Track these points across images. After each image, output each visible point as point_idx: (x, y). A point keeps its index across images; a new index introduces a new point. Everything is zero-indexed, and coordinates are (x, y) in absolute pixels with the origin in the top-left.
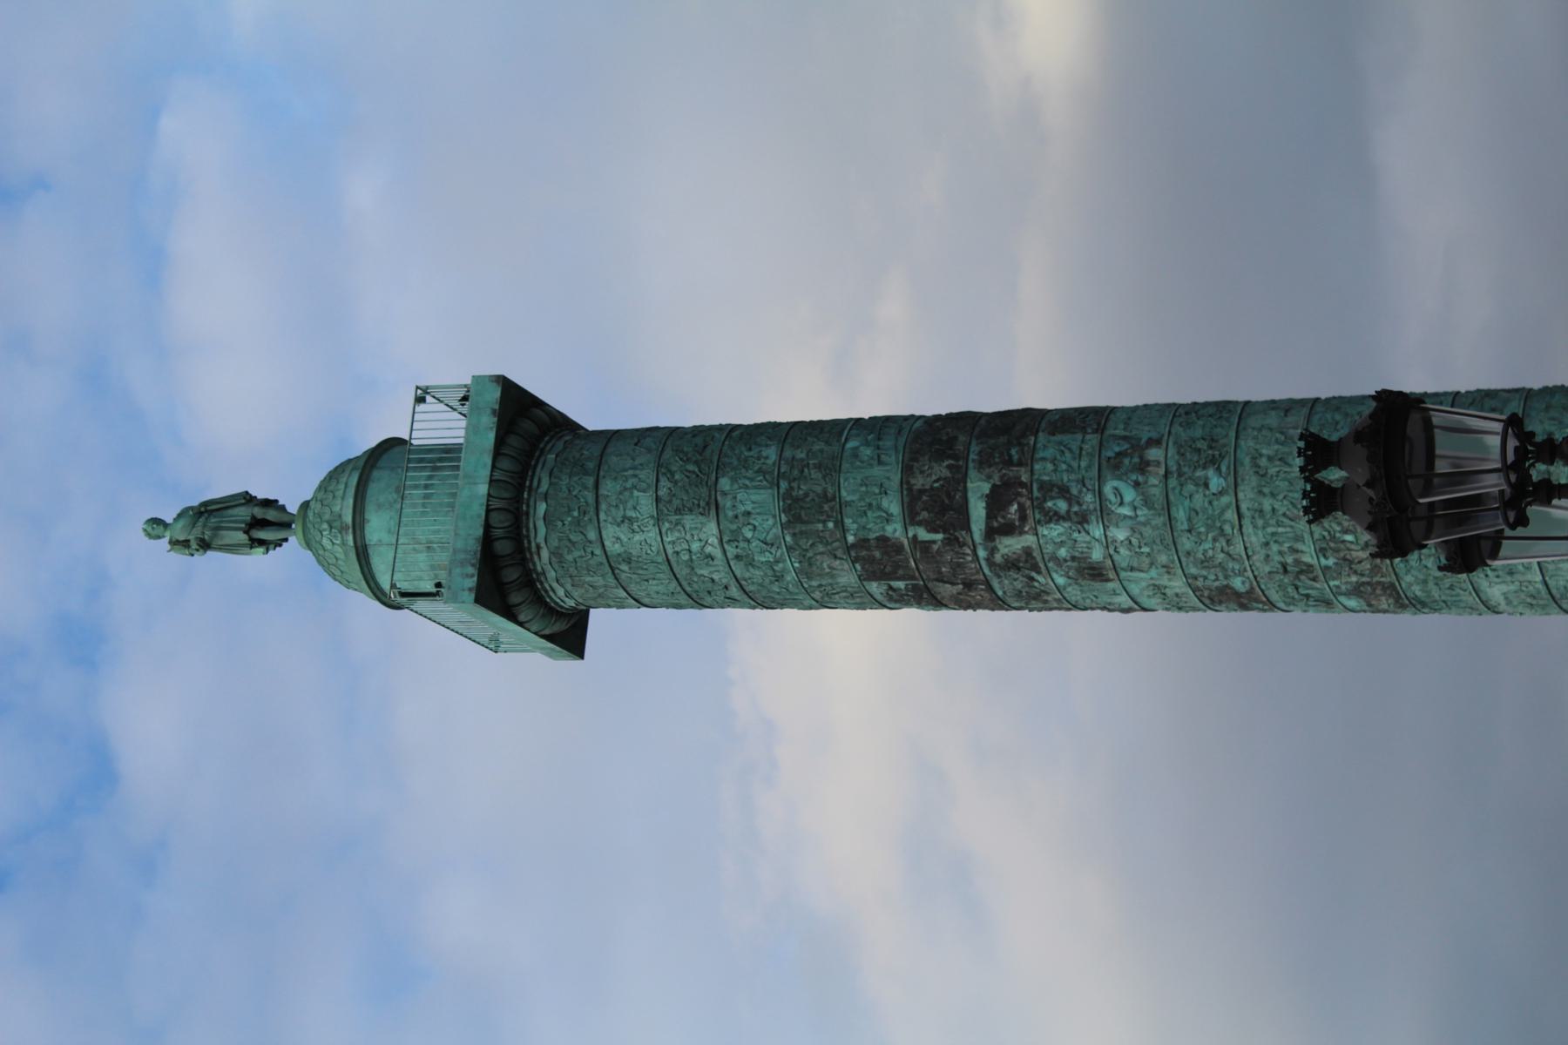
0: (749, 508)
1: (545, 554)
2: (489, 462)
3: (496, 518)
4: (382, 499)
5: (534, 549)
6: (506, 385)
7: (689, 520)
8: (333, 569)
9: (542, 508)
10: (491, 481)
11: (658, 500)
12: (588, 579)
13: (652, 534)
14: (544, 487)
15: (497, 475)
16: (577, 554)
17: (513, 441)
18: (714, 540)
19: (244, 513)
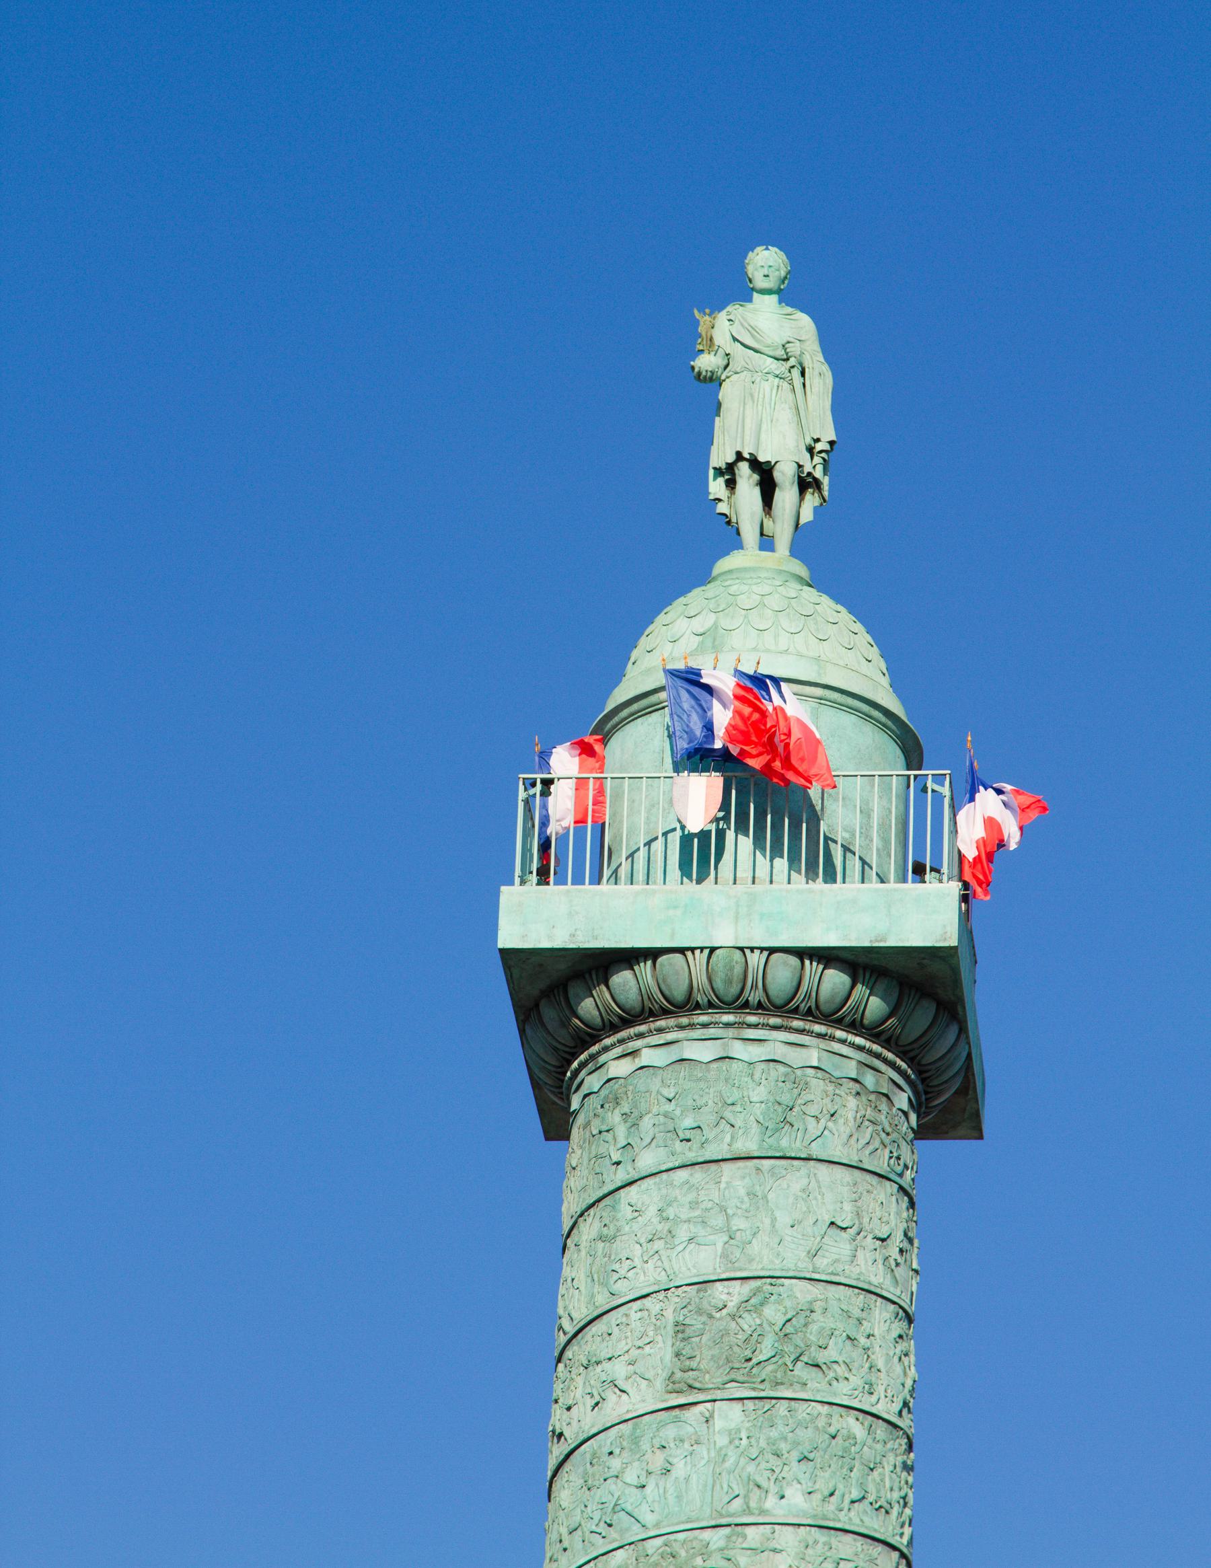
0: (680, 1469)
7: (662, 1352)
9: (702, 1052)
10: (742, 949)
14: (739, 1050)
15: (755, 959)
17: (835, 980)
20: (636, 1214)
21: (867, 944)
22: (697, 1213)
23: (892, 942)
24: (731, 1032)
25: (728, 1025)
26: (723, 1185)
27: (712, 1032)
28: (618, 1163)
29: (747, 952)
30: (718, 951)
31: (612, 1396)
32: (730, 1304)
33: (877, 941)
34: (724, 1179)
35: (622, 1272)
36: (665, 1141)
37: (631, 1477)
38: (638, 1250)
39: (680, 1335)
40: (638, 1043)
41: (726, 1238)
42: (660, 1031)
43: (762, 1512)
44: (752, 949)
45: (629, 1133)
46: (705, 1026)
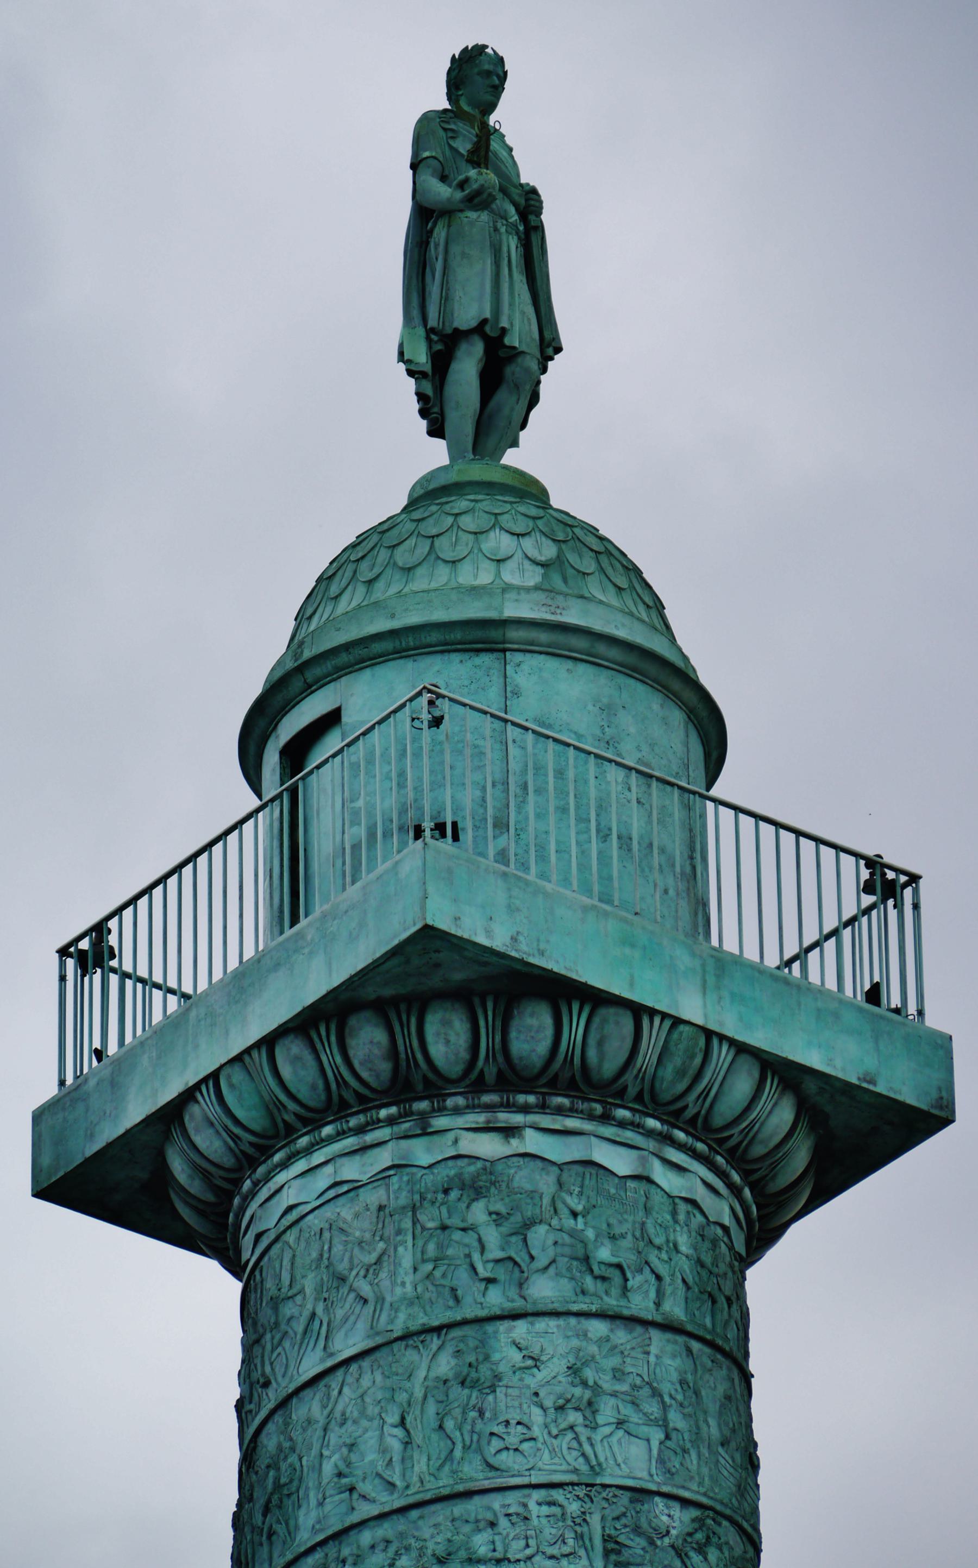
1: (489, 1146)
3: (619, 1028)
4: (626, 721)
5: (505, 1118)
6: (917, 1123)
8: (375, 538)
9: (620, 1162)
10: (709, 1034)
11: (640, 1494)
12: (406, 1257)
13: (552, 1462)
15: (722, 1055)
16: (492, 1236)
19: (520, 331)
21: (854, 1081)
22: (625, 1387)
23: (880, 1088)
24: (651, 1145)
25: (650, 1133)
28: (490, 1281)
29: (715, 1042)
30: (682, 1027)
32: (674, 1532)
33: (865, 1080)
34: (654, 1350)
35: (512, 1440)
36: (569, 1269)
38: (537, 1416)
39: (613, 1557)
40: (518, 1119)
41: (662, 1436)
44: (722, 1038)
46: (622, 1124)
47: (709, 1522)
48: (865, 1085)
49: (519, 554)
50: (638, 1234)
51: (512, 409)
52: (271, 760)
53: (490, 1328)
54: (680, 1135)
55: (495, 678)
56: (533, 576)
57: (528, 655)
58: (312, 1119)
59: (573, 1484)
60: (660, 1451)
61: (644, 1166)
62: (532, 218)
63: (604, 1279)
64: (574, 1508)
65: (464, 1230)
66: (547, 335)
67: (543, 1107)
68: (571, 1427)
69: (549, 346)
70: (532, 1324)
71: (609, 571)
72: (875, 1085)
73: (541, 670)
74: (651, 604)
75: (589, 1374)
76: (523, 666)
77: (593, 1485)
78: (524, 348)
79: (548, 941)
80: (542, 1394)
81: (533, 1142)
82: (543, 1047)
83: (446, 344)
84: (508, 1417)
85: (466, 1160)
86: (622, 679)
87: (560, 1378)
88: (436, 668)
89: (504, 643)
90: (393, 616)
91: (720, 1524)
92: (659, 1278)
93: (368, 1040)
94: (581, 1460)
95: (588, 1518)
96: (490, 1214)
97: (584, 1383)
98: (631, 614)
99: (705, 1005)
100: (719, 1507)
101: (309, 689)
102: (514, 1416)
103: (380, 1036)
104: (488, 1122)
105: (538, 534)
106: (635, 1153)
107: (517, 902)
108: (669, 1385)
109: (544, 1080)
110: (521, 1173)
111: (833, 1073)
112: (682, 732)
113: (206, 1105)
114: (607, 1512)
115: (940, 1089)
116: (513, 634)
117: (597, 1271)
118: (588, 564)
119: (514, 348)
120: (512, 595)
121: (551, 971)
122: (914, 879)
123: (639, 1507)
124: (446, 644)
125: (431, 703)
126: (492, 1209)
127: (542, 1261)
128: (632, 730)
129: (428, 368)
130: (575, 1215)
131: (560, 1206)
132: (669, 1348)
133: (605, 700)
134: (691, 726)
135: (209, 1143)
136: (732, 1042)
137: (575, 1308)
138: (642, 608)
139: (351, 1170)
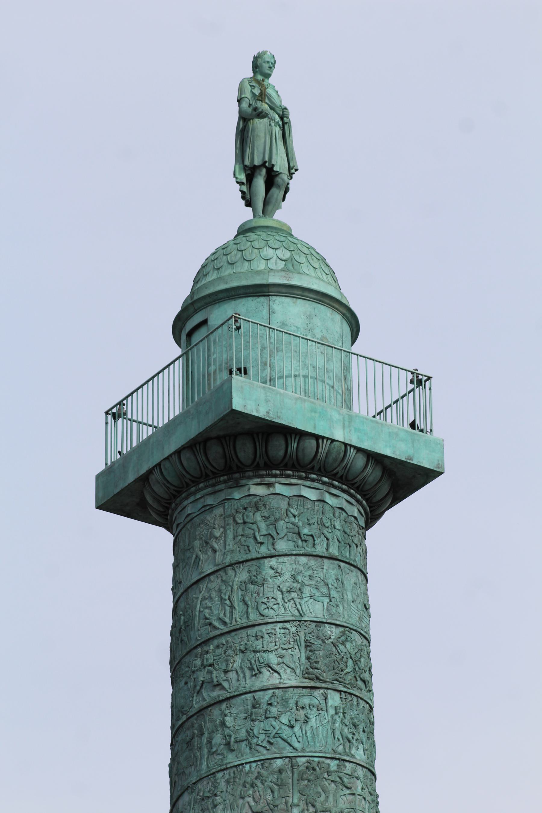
0: (313, 722)
1: (260, 491)
2: (366, 445)
4: (317, 321)
7: (299, 655)
9: (312, 495)
10: (346, 445)
11: (319, 623)
15: (352, 452)
18: (275, 680)
19: (280, 164)
20: (277, 574)
21: (404, 459)
22: (313, 582)
23: (415, 462)
24: (325, 488)
25: (324, 483)
26: (325, 571)
27: (316, 485)
28: (262, 543)
29: (348, 447)
30: (335, 443)
31: (266, 673)
32: (332, 637)
33: (408, 459)
34: (325, 567)
36: (292, 537)
37: (284, 719)
39: (309, 648)
40: (273, 480)
41: (328, 600)
42: (288, 476)
43: (353, 756)
44: (351, 446)
45: (268, 528)
46: (313, 480)
47: (347, 632)
48: (408, 461)
49: (275, 257)
50: (319, 522)
51: (278, 195)
52: (184, 337)
53: (261, 561)
54: (336, 483)
55: (265, 306)
56: (281, 265)
57: (278, 297)
58: (196, 481)
59: (293, 621)
60: (327, 606)
61: (322, 496)
62: (285, 119)
63: (306, 541)
64: (293, 630)
65: (252, 523)
66: (292, 165)
67: (281, 476)
68: (293, 599)
69: (292, 170)
70: (278, 559)
71: (311, 262)
72: (412, 460)
73: (283, 303)
74: (328, 272)
75: (300, 578)
76: (276, 302)
77: (301, 621)
78: (281, 171)
79: (281, 413)
80: (281, 587)
81: (279, 489)
82: (281, 453)
83: (251, 171)
84: (268, 596)
85: (253, 497)
86: (315, 305)
87: (288, 580)
88: (243, 303)
89: (268, 293)
90: (227, 283)
91: (351, 633)
92: (328, 539)
93: (215, 451)
94: (296, 611)
95: (299, 633)
96: (262, 517)
97: (298, 582)
98: (319, 278)
99: (344, 434)
100: (351, 627)
101: (196, 311)
102: (271, 595)
103: (220, 450)
104: (261, 481)
105: (283, 248)
106: (318, 491)
107: (269, 398)
108: (331, 580)
109: (282, 465)
110: (274, 501)
111: (395, 457)
112: (339, 323)
113: (156, 475)
114: (306, 631)
115: (438, 460)
116: (272, 289)
117: (303, 538)
118: (303, 259)
119: (278, 172)
120: (272, 274)
121: (282, 424)
122: (429, 378)
123: (319, 628)
124: (246, 294)
125: (236, 321)
126: (262, 515)
127: (282, 535)
128: (319, 324)
129: (244, 181)
130: (294, 516)
131: (289, 513)
132: (332, 566)
133: (308, 313)
134: (344, 320)
135: (159, 490)
136: (355, 447)
137: (294, 553)
138: (324, 275)
139: (210, 501)
